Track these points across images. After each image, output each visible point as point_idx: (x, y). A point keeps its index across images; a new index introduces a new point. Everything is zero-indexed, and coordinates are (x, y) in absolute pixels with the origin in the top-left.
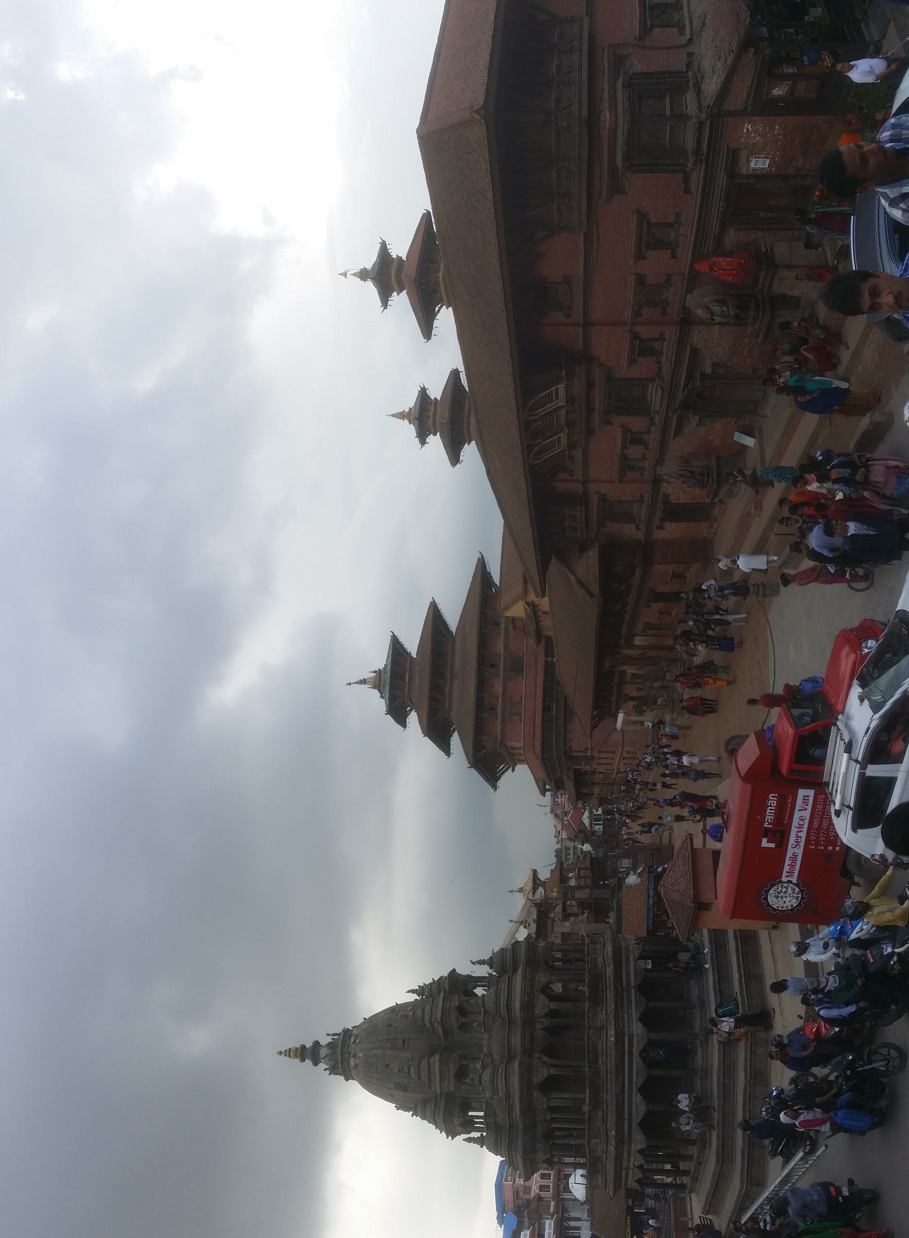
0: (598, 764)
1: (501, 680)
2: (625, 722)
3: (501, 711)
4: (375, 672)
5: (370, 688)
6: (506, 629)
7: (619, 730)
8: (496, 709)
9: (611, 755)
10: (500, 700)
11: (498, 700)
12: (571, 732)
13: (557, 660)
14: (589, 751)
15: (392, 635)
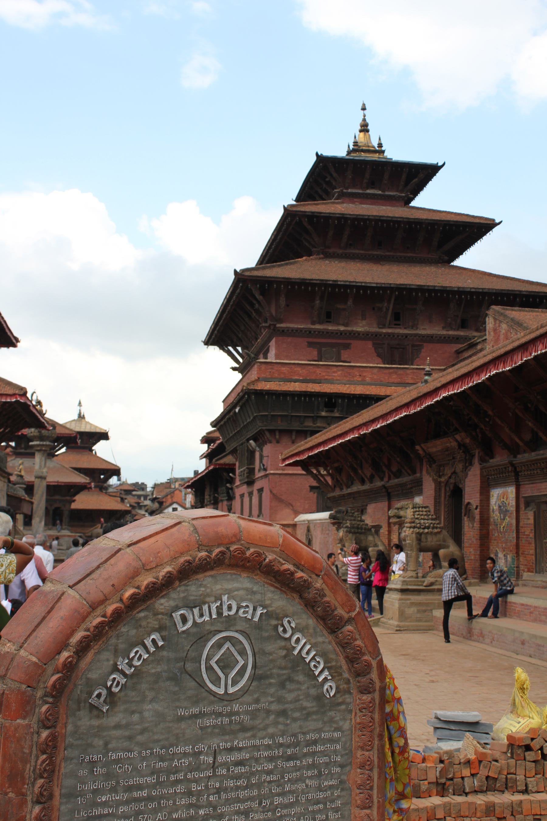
0: (242, 496)
1: (374, 329)
2: (309, 527)
3: (326, 329)
4: (380, 145)
5: (355, 137)
6: (457, 340)
7: (296, 520)
8: (327, 322)
9: (255, 511)
10: (342, 328)
11: (343, 325)
12: (293, 442)
13: (426, 382)
14: (262, 473)
15: (440, 164)
